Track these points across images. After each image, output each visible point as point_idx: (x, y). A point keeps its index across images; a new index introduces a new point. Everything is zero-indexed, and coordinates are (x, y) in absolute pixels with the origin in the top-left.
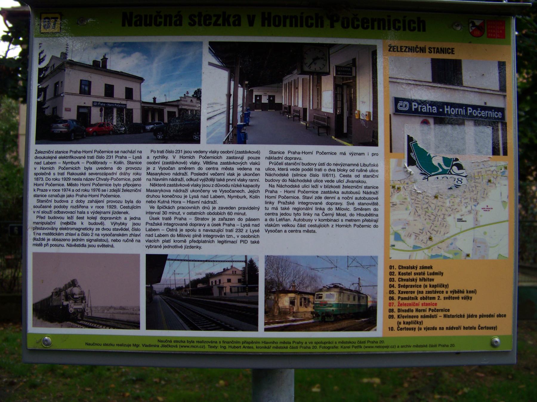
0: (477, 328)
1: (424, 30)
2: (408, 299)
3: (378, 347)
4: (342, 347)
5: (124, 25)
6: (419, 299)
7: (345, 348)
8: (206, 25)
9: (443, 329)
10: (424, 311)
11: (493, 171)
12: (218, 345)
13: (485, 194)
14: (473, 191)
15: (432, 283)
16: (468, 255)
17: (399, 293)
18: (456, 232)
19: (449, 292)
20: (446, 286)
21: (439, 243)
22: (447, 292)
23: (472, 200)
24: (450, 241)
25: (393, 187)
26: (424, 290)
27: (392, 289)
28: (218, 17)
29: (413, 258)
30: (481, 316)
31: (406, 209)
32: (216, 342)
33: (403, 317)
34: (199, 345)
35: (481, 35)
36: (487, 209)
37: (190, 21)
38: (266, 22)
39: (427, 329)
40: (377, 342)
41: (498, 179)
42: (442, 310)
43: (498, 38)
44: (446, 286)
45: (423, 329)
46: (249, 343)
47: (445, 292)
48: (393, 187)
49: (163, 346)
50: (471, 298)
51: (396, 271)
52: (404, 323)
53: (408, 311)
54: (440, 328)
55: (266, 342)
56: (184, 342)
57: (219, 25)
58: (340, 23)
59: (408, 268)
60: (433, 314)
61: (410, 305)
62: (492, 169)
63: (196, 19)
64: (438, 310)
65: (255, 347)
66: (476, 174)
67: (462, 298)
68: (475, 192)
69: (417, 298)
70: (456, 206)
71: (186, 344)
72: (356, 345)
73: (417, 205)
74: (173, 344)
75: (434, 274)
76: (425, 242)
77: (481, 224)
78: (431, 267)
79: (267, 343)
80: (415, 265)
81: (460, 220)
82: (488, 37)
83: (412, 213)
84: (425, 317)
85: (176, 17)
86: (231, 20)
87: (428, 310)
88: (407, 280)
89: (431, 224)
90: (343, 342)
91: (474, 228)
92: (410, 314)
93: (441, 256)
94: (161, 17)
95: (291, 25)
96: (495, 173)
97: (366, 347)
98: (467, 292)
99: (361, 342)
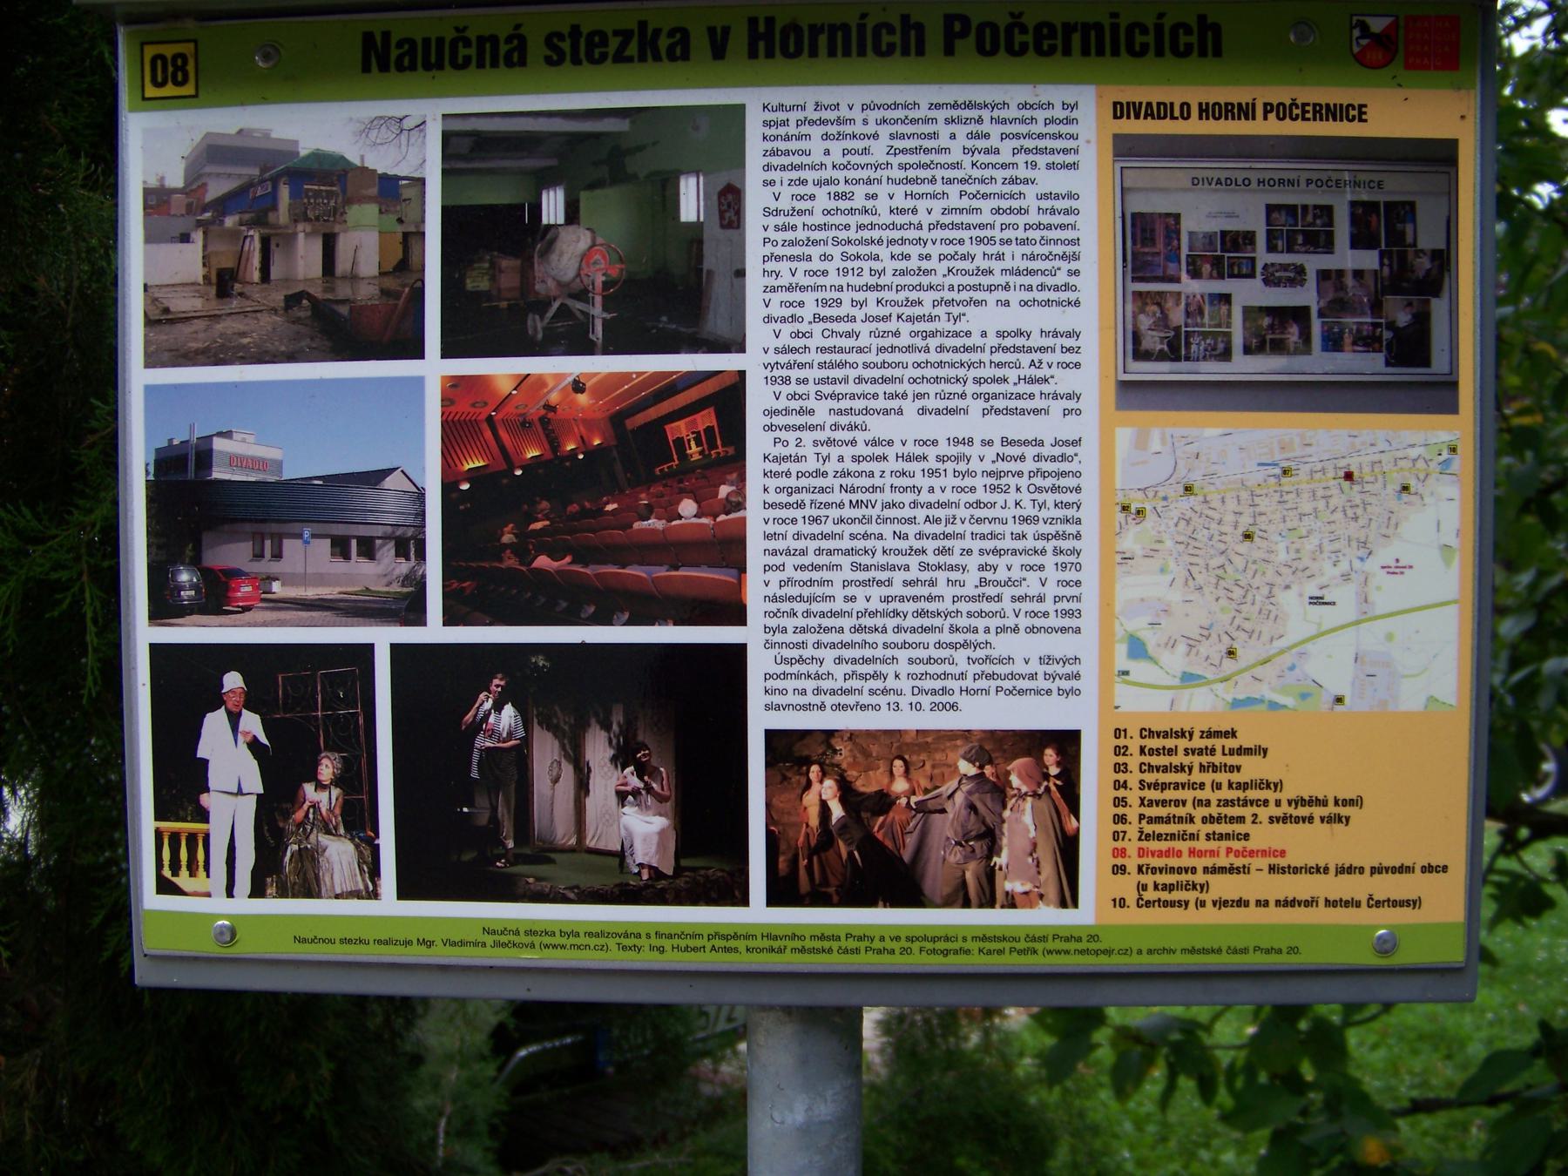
0: (1364, 904)
1: (1218, 53)
2: (1167, 820)
3: (1081, 952)
4: (980, 951)
5: (366, 69)
6: (1198, 820)
7: (990, 952)
9: (1266, 904)
10: (1213, 853)
11: (1415, 460)
12: (643, 942)
13: (1392, 523)
14: (1356, 519)
15: (1236, 777)
16: (1339, 700)
17: (1142, 804)
18: (1308, 635)
19: (1284, 803)
20: (1276, 786)
21: (1254, 666)
22: (1278, 803)
23: (1354, 544)
24: (1288, 659)
25: (1125, 508)
26: (1214, 797)
27: (1121, 793)
29: (1182, 707)
30: (1374, 870)
31: (1162, 571)
32: (639, 936)
33: (1154, 870)
34: (593, 941)
36: (1396, 569)
37: (549, 53)
38: (761, 45)
39: (1221, 903)
40: (1079, 939)
41: (1431, 481)
42: (1264, 853)
43: (1436, 68)
44: (1276, 786)
45: (1209, 904)
46: (726, 937)
47: (1272, 803)
48: (1125, 508)
49: (497, 944)
50: (1348, 819)
51: (1134, 744)
52: (1156, 887)
53: (1167, 853)
54: (1258, 903)
55: (774, 938)
56: (553, 934)
57: (630, 60)
58: (972, 38)
59: (1166, 735)
60: (1239, 862)
61: (1173, 836)
62: (1413, 453)
63: (566, 46)
64: (1252, 853)
65: (742, 949)
66: (1366, 470)
67: (1322, 820)
68: (1361, 522)
69: (1191, 820)
70: (1306, 562)
71: (557, 940)
72: (1022, 945)
73: (1194, 560)
74: (523, 939)
75: (1241, 751)
76: (1217, 662)
77: (1378, 612)
78: (1233, 734)
79: (776, 938)
80: (1187, 728)
81: (1317, 601)
82: (1408, 67)
83: (1180, 582)
84: (1215, 870)
85: (509, 40)
86: (664, 43)
87: (1223, 852)
88: (1165, 769)
89: (1233, 613)
90: (984, 938)
91: (1358, 622)
93: (1262, 701)
94: (467, 43)
95: (832, 53)
96: (1420, 464)
97: (1050, 952)
98: (1336, 803)
99: (1034, 939)
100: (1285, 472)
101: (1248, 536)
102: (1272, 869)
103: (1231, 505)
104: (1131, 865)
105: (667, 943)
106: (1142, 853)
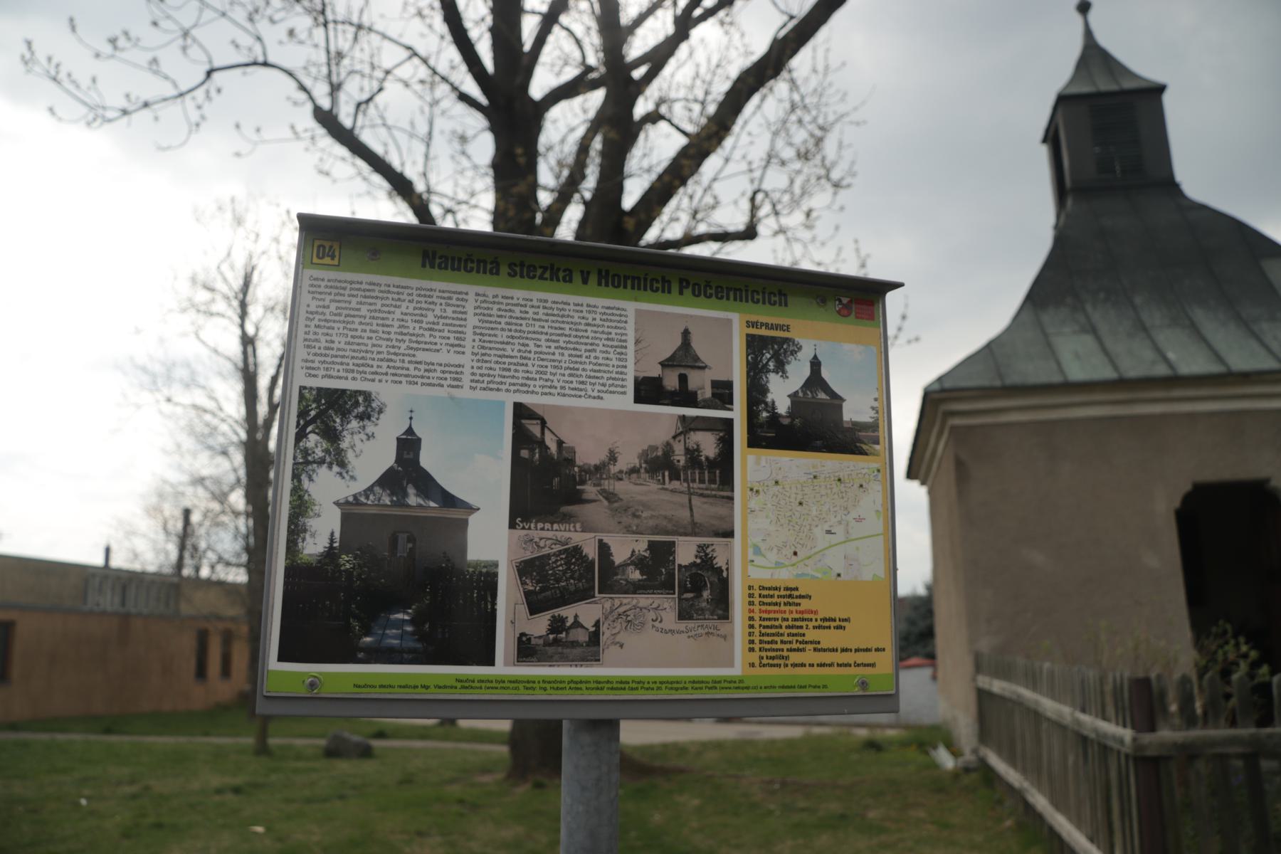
1: (786, 305)
2: (771, 627)
8: (529, 277)
10: (791, 642)
12: (536, 685)
16: (839, 575)
26: (790, 617)
28: (545, 269)
29: (776, 577)
35: (849, 315)
36: (859, 520)
39: (795, 665)
42: (811, 642)
49: (463, 687)
51: (757, 593)
53: (772, 642)
59: (769, 589)
60: (801, 646)
61: (773, 635)
63: (518, 269)
71: (494, 685)
81: (829, 532)
86: (561, 274)
88: (770, 604)
92: (774, 646)
94: (472, 262)
100: (815, 477)
101: (801, 504)
102: (815, 650)
103: (794, 490)
104: (757, 649)
105: (548, 686)
106: (761, 642)
